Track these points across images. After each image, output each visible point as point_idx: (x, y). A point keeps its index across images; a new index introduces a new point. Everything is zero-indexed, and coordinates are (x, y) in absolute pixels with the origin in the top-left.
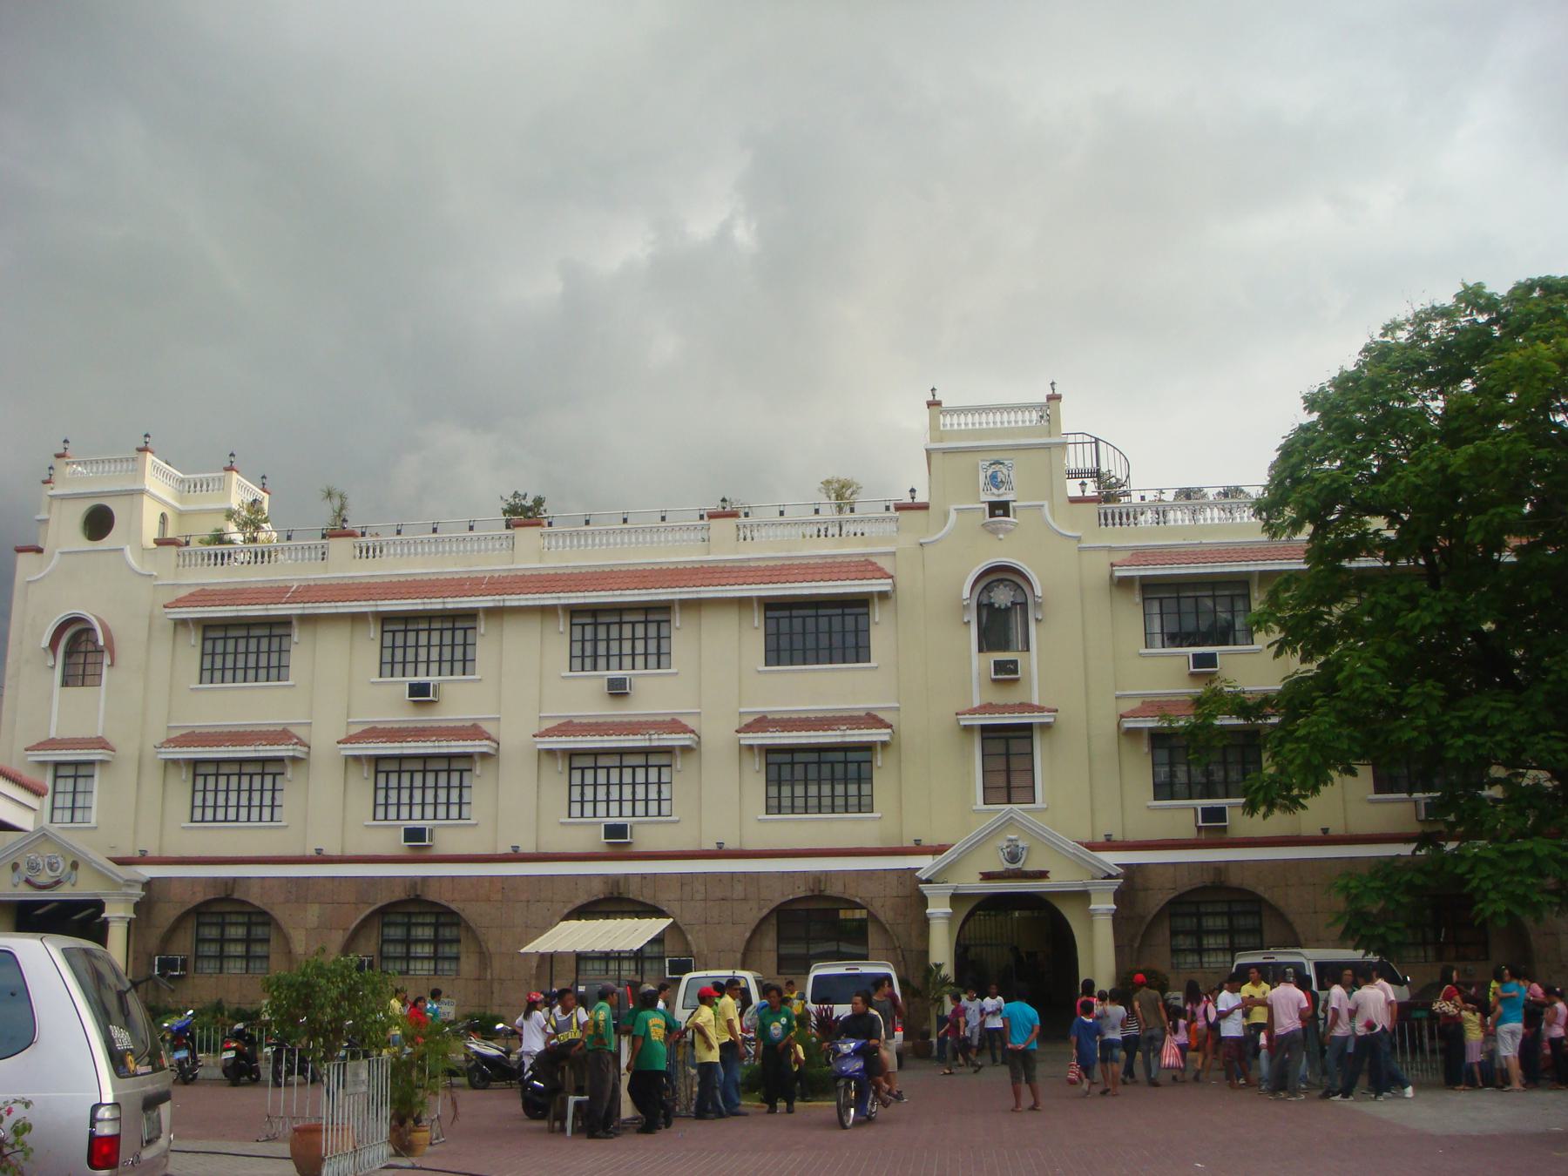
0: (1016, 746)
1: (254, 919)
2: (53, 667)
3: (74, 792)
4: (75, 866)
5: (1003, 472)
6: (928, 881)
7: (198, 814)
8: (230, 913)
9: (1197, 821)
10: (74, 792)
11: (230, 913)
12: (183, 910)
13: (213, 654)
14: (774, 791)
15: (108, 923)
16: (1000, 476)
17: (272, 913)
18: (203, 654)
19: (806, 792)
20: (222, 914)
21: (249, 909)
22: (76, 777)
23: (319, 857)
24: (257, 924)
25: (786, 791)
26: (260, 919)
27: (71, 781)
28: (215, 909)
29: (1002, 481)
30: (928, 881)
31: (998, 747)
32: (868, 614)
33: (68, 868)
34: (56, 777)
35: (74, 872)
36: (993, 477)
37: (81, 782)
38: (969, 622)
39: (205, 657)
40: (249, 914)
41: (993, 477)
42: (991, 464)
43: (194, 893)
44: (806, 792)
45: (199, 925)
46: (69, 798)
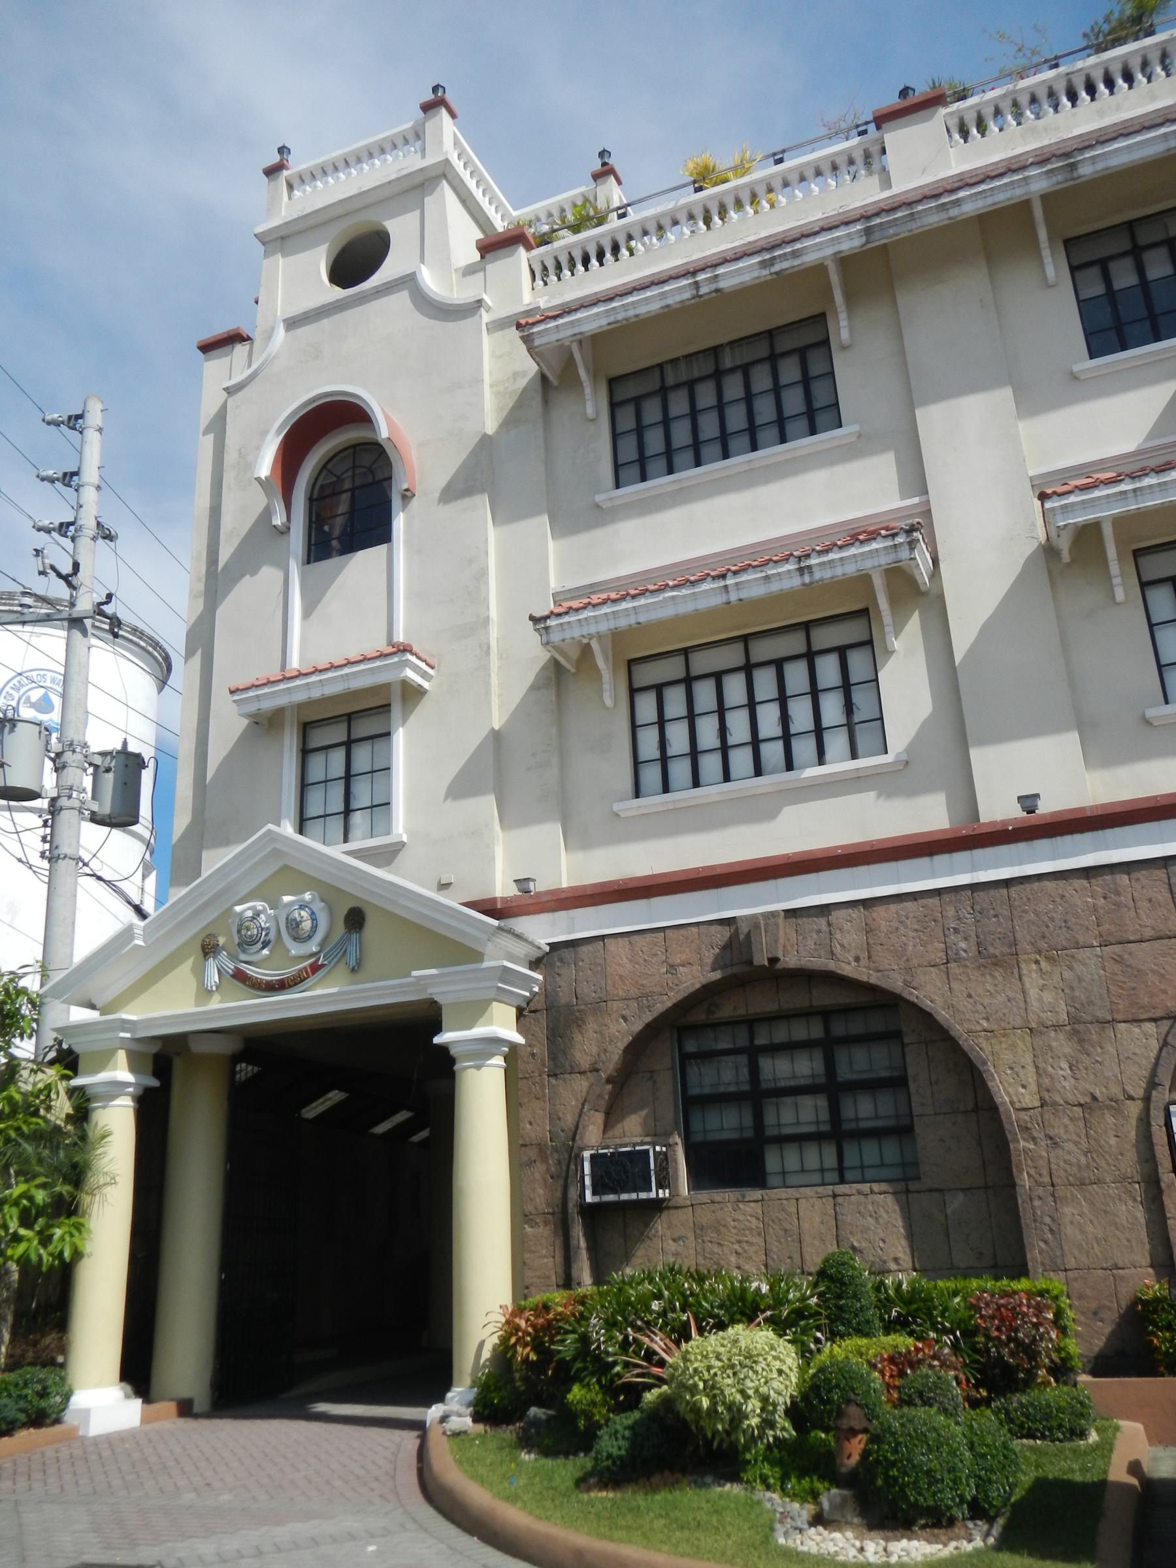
1: (839, 1028)
2: (284, 531)
3: (348, 777)
4: (355, 919)
7: (652, 775)
8: (771, 1019)
10: (348, 777)
11: (771, 1019)
12: (648, 1017)
13: (639, 431)
15: (452, 1061)
17: (912, 995)
18: (615, 436)
20: (751, 1023)
21: (824, 998)
22: (348, 745)
23: (1033, 819)
24: (851, 1040)
26: (857, 1026)
27: (337, 758)
28: (726, 1011)
33: (340, 929)
34: (305, 753)
35: (354, 936)
37: (362, 757)
39: (621, 443)
40: (825, 1015)
43: (672, 968)
45: (685, 1059)
46: (338, 791)
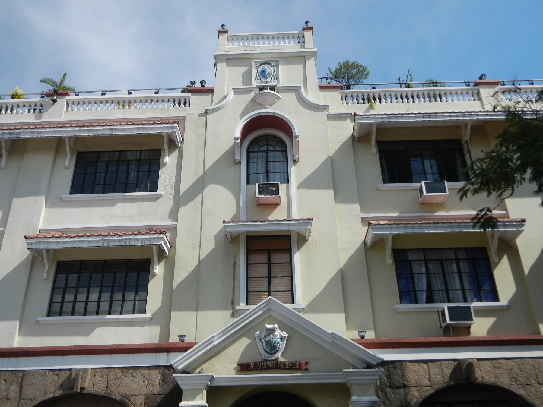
0: (276, 258)
5: (269, 69)
6: (184, 372)
9: (444, 320)
14: (58, 298)
16: (267, 71)
19: (88, 297)
25: (69, 297)
29: (269, 74)
30: (184, 372)
31: (263, 258)
32: (160, 159)
36: (263, 72)
38: (240, 163)
41: (263, 72)
42: (260, 65)
44: (88, 297)
